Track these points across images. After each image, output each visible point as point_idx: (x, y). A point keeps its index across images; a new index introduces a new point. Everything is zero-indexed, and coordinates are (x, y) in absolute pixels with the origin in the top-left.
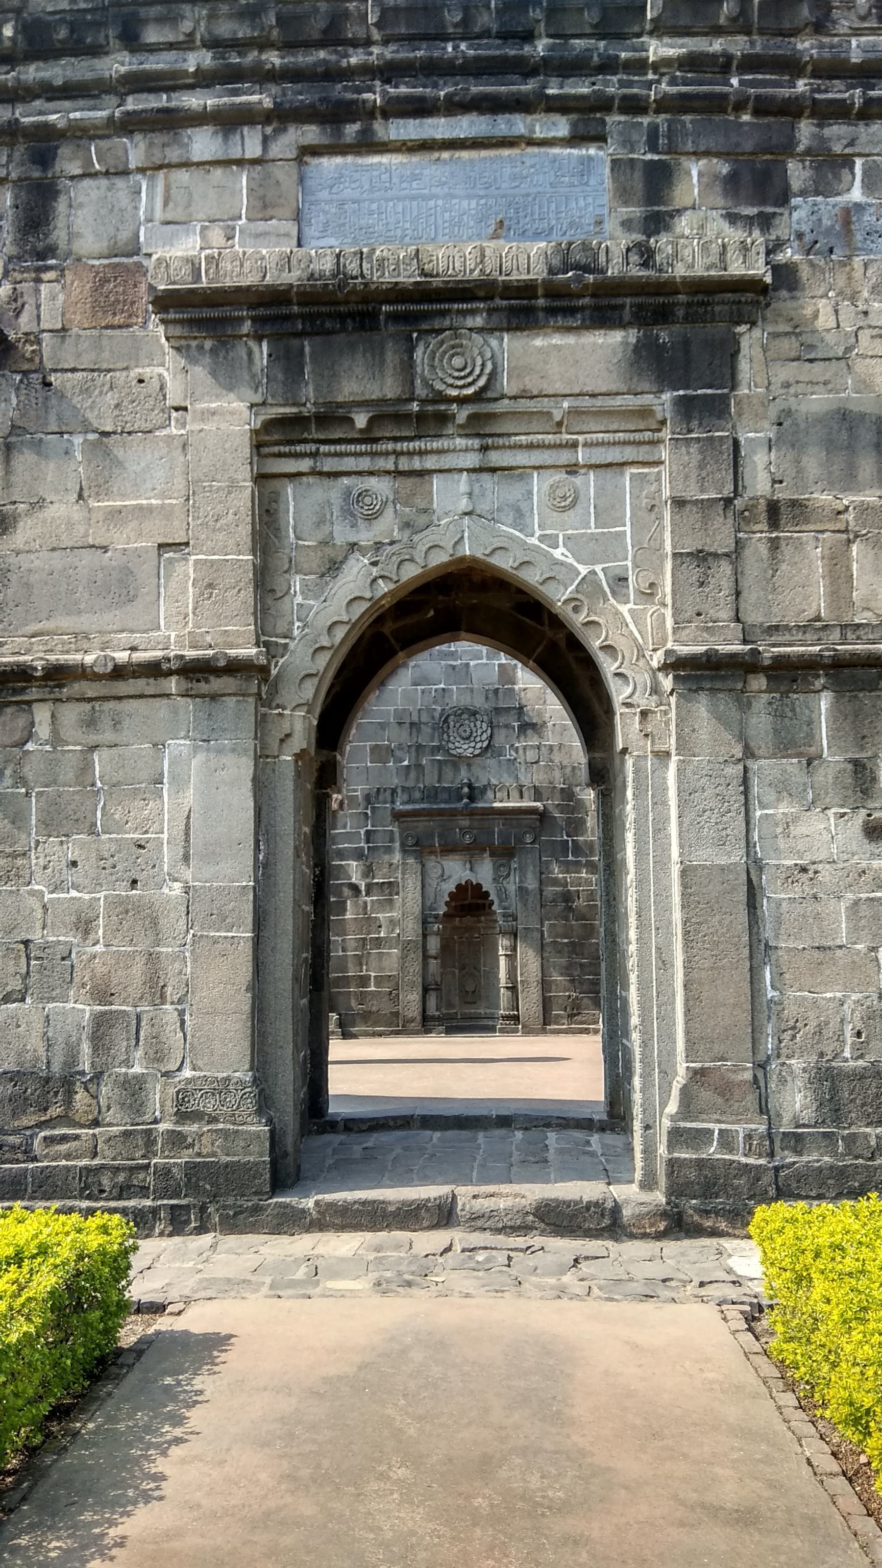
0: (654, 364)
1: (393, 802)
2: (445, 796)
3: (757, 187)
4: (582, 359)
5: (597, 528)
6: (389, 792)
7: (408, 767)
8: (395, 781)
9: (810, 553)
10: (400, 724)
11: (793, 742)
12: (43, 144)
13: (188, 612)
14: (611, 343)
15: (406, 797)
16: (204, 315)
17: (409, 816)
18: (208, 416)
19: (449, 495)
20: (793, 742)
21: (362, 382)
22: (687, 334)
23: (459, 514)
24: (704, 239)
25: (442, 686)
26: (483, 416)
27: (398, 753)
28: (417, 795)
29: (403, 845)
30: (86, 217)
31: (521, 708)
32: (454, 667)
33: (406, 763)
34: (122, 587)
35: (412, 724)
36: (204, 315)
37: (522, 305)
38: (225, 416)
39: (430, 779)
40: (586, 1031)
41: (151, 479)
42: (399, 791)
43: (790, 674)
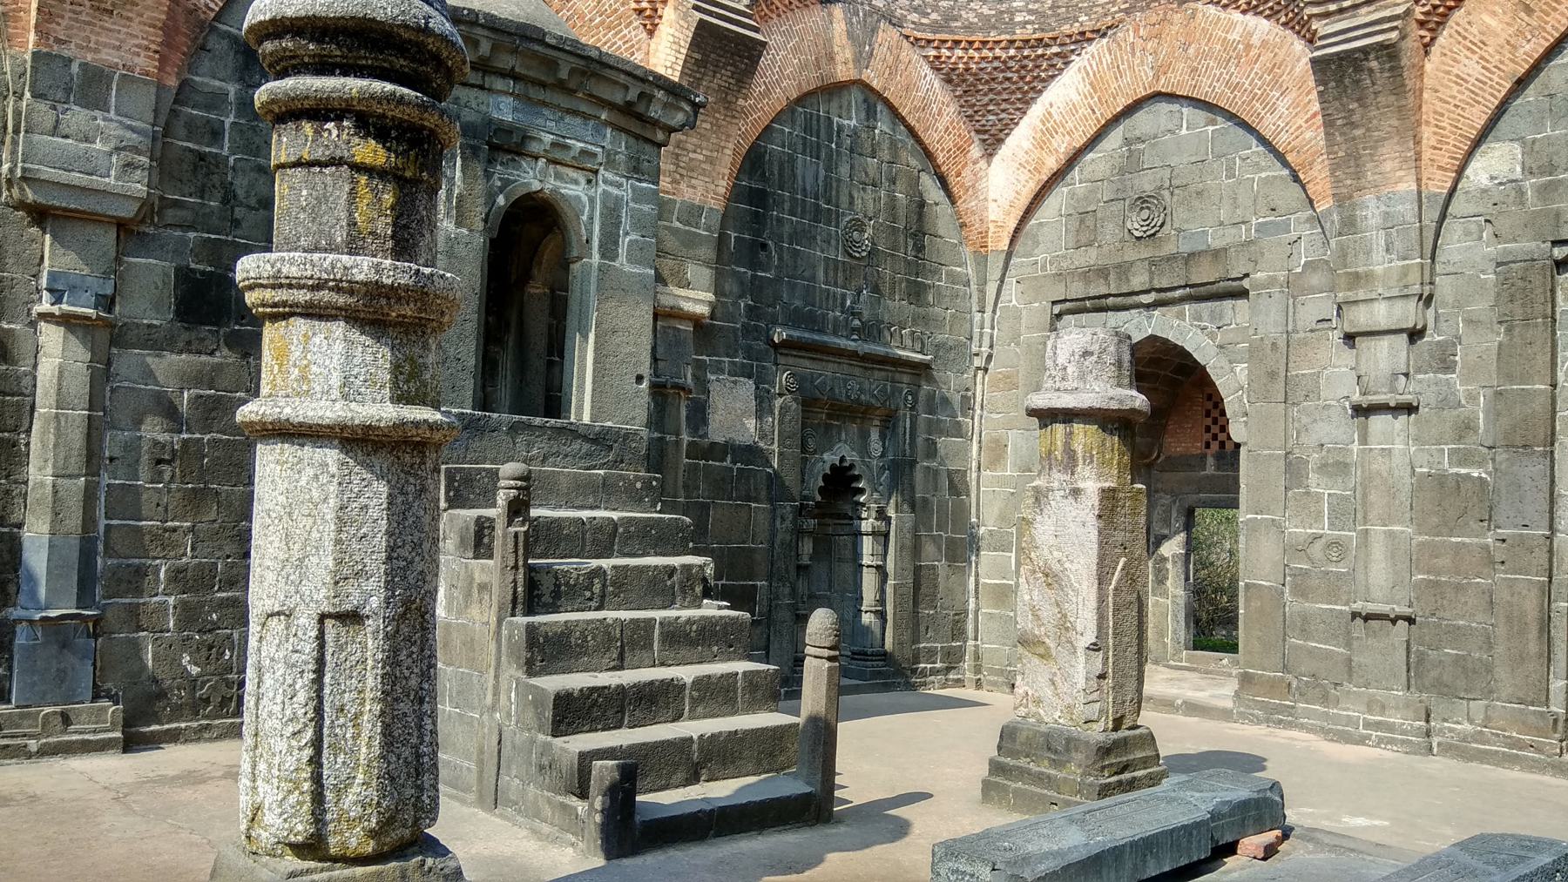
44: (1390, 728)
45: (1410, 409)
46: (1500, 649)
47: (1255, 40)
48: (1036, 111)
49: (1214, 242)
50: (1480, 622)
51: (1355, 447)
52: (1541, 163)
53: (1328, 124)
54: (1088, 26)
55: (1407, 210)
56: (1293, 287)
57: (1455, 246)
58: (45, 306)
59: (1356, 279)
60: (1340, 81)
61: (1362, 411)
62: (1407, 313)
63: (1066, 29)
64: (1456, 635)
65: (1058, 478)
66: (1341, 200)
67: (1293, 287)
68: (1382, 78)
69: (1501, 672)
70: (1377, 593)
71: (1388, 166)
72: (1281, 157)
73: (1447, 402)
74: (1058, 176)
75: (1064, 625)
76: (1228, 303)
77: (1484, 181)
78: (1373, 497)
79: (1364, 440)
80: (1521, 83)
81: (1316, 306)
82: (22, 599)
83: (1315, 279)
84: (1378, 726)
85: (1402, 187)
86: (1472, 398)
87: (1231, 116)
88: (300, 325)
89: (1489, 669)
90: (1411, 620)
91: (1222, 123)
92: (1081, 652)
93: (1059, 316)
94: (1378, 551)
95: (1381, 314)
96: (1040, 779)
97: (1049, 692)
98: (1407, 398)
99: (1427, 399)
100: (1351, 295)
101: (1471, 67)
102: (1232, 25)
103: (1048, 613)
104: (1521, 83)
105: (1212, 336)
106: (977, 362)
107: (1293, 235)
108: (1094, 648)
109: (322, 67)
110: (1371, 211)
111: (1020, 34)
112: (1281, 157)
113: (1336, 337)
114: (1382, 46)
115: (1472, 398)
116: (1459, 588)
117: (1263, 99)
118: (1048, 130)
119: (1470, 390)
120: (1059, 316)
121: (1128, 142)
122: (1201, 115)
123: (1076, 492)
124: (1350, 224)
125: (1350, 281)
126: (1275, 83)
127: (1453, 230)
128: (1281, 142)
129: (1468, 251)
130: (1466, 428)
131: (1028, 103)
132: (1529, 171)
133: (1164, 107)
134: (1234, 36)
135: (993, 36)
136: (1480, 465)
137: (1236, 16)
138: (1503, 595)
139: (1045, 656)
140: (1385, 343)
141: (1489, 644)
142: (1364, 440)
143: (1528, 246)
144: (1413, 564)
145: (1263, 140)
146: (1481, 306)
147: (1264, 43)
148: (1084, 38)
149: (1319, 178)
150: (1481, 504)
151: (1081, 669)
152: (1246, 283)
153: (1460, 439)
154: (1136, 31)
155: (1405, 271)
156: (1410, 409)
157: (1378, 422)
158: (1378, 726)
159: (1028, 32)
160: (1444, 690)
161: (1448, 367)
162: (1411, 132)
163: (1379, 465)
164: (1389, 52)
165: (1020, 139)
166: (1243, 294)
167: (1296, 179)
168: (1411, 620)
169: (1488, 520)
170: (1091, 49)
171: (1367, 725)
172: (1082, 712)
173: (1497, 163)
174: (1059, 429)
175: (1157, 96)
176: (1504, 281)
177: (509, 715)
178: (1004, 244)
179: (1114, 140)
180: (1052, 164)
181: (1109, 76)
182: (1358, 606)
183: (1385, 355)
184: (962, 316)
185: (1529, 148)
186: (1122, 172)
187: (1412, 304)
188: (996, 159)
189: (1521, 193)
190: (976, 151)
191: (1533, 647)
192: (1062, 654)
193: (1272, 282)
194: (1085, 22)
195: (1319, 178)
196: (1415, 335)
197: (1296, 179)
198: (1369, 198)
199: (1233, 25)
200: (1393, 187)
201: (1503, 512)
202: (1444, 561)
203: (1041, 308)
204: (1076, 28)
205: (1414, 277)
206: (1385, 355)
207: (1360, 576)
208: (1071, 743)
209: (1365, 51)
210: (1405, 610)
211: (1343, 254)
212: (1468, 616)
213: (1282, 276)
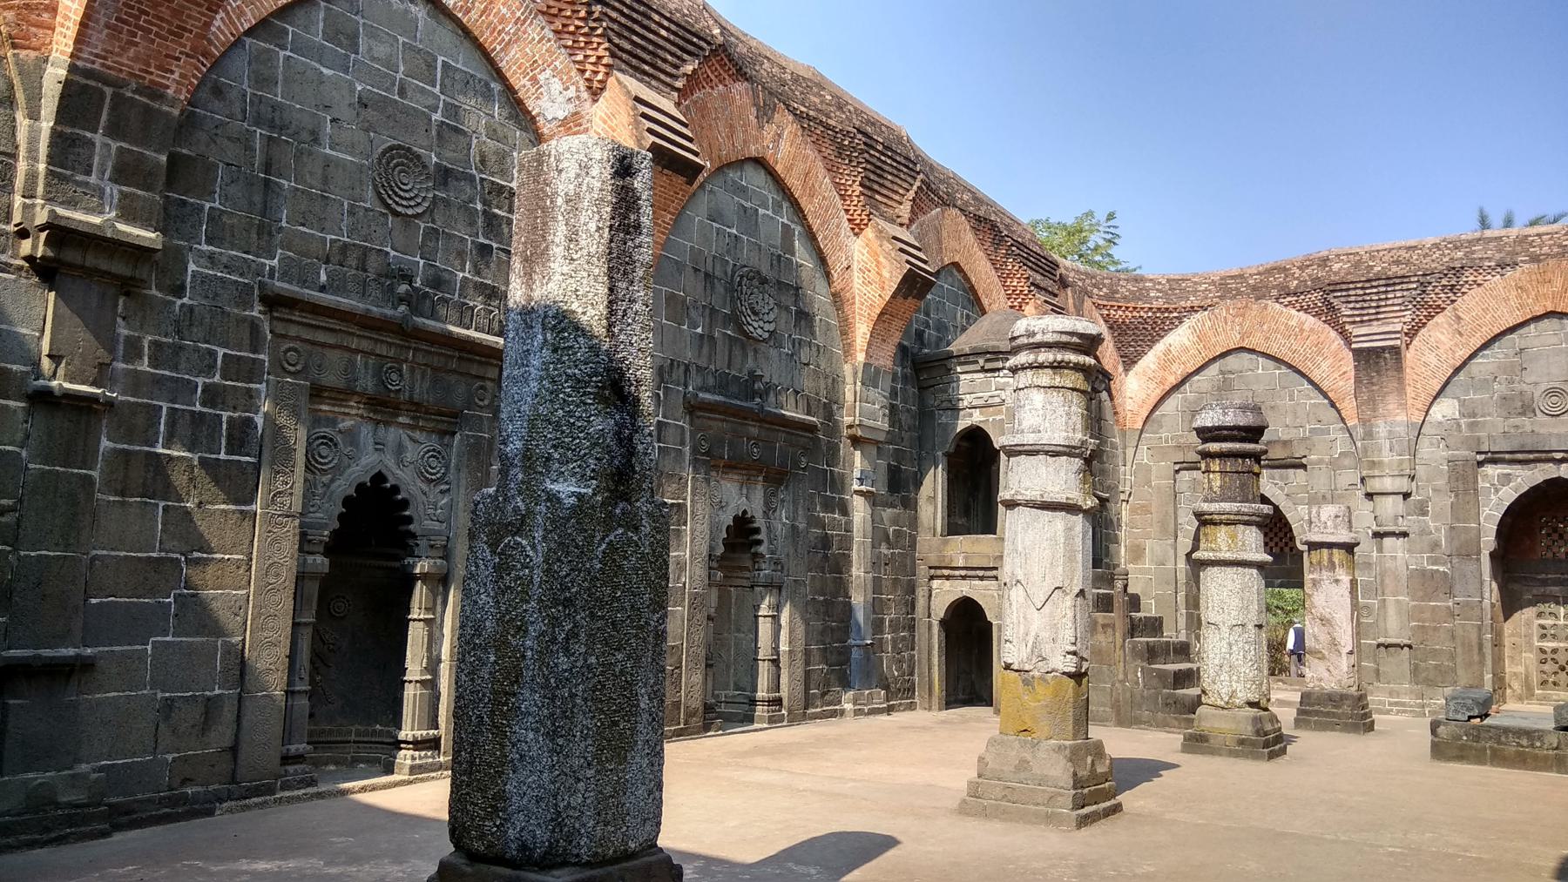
1: (686, 386)
2: (734, 389)
6: (682, 368)
7: (701, 336)
8: (689, 355)
10: (696, 270)
15: (699, 381)
17: (711, 411)
25: (734, 231)
27: (693, 313)
28: (711, 381)
29: (695, 451)
31: (797, 289)
32: (745, 209)
33: (699, 330)
35: (707, 275)
39: (720, 363)
40: (834, 714)
42: (693, 369)
44: (1403, 704)
45: (1405, 535)
46: (1459, 660)
47: (1306, 327)
48: (1160, 347)
49: (1285, 437)
50: (1446, 646)
51: (1375, 554)
52: (1469, 411)
53: (1358, 381)
54: (1196, 303)
55: (1401, 430)
56: (1334, 465)
57: (1426, 450)
58: (856, 487)
59: (1373, 464)
60: (1367, 361)
61: (1377, 535)
62: (1403, 484)
63: (1183, 303)
64: (1435, 653)
65: (1325, 574)
66: (1364, 422)
67: (1334, 465)
68: (1391, 363)
69: (1460, 672)
70: (1391, 633)
71: (1391, 407)
72: (1325, 395)
73: (1424, 532)
74: (1176, 387)
75: (1334, 643)
76: (1291, 471)
77: (1439, 417)
78: (1387, 581)
79: (1380, 550)
80: (1457, 371)
81: (1349, 477)
82: (853, 635)
83: (1347, 462)
84: (1396, 704)
85: (1399, 418)
86: (1438, 529)
87: (1290, 366)
88: (1242, 527)
89: (1454, 670)
90: (1410, 647)
91: (1284, 370)
92: (1344, 657)
93: (1177, 472)
94: (1391, 610)
95: (1388, 484)
96: (1328, 714)
97: (1326, 674)
98: (1404, 529)
99: (1413, 529)
100: (1371, 473)
101: (1432, 359)
102: (1291, 317)
103: (1324, 638)
104: (1457, 371)
105: (1282, 489)
106: (1122, 497)
107: (1332, 436)
108: (1351, 653)
109: (1242, 440)
110: (1381, 429)
111: (1155, 305)
112: (1325, 395)
113: (1360, 494)
114: (1392, 347)
115: (1438, 529)
116: (1435, 629)
117: (1312, 360)
118: (1167, 361)
119: (1437, 526)
120: (1177, 472)
121: (1222, 372)
122: (1271, 364)
123: (1337, 581)
124: (1369, 435)
125: (1368, 465)
126: (1319, 353)
127: (1424, 443)
128: (1325, 386)
129: (1432, 453)
130: (1435, 545)
131: (1154, 341)
132: (1463, 415)
133: (1246, 356)
134: (1293, 323)
135: (1140, 304)
136: (1444, 564)
137: (1293, 312)
138: (1460, 632)
139: (1323, 658)
140: (1390, 499)
141: (1453, 657)
142: (1380, 550)
143: (1464, 453)
144: (1411, 618)
145: (1311, 382)
146: (1441, 482)
147: (1312, 330)
148: (1193, 309)
149: (1349, 407)
150: (1445, 585)
151: (1344, 663)
152: (1304, 461)
153: (1432, 551)
154: (1228, 310)
155: (1401, 462)
156: (1405, 535)
157: (1387, 541)
158: (1396, 704)
159: (1160, 303)
160: (1431, 683)
161: (1425, 513)
162: (1401, 390)
163: (1389, 564)
164: (1395, 351)
165: (1150, 361)
166: (1304, 467)
167: (1333, 405)
168: (1410, 647)
169: (1450, 593)
170: (1198, 316)
171: (1390, 704)
172: (1345, 682)
173: (1445, 409)
174: (1325, 551)
175: (1242, 349)
176: (1452, 470)
177: (1137, 683)
178: (1139, 425)
179: (1214, 370)
180: (1172, 380)
181: (1210, 333)
182: (1381, 640)
183: (1390, 506)
184: (1116, 471)
185: (1462, 403)
186: (1219, 389)
187: (1406, 479)
188: (1131, 373)
189: (1459, 425)
190: (1121, 369)
191: (1476, 658)
192: (1333, 657)
193: (1320, 462)
194: (1193, 301)
195: (1349, 407)
196: (1406, 496)
197: (1333, 405)
198: (1380, 422)
199: (1291, 317)
200: (1395, 417)
201: (1458, 588)
202: (1427, 615)
203: (1167, 466)
204: (1189, 304)
205: (1406, 465)
206: (1390, 506)
207: (1381, 624)
208: (1343, 697)
209: (1383, 349)
210: (1407, 641)
211: (1365, 449)
212: (1441, 644)
213: (1327, 458)
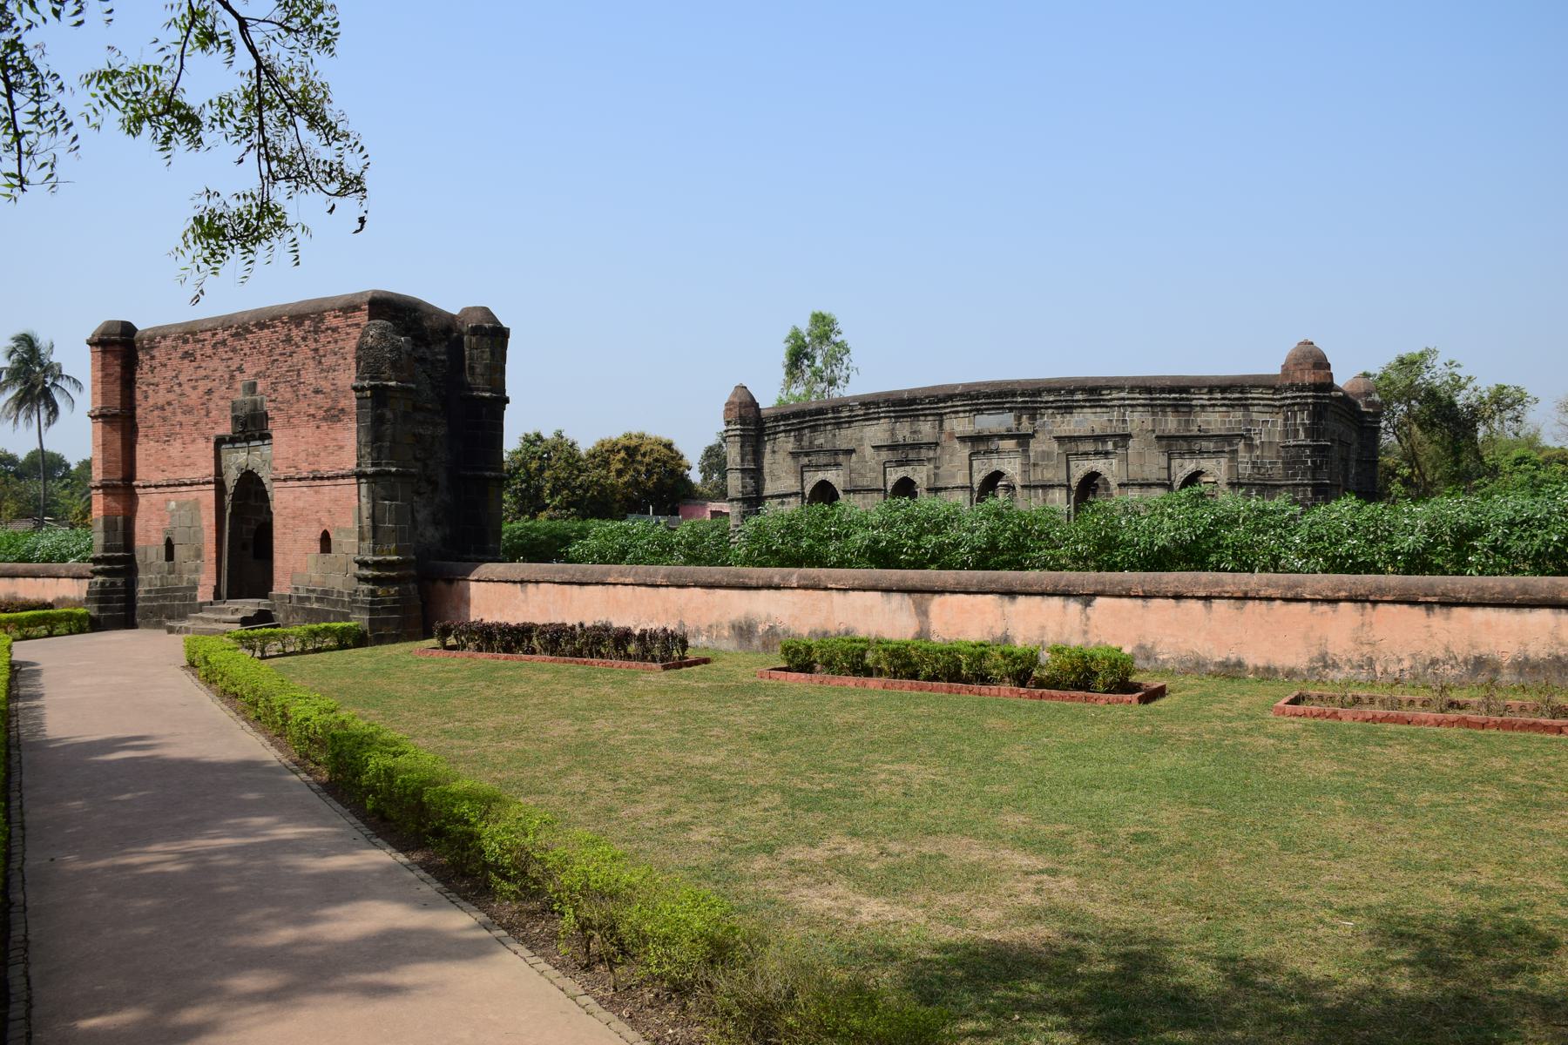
0: (1019, 444)
3: (1033, 418)
4: (1009, 444)
5: (1012, 467)
9: (1039, 470)
11: (1036, 496)
12: (941, 415)
13: (961, 479)
14: (1014, 442)
16: (962, 439)
18: (964, 451)
19: (994, 462)
20: (1036, 496)
21: (982, 448)
22: (1023, 440)
23: (996, 464)
24: (1026, 426)
26: (997, 451)
30: (947, 425)
34: (953, 476)
36: (962, 439)
37: (1002, 437)
38: (967, 452)
41: (957, 463)
43: (1035, 487)
